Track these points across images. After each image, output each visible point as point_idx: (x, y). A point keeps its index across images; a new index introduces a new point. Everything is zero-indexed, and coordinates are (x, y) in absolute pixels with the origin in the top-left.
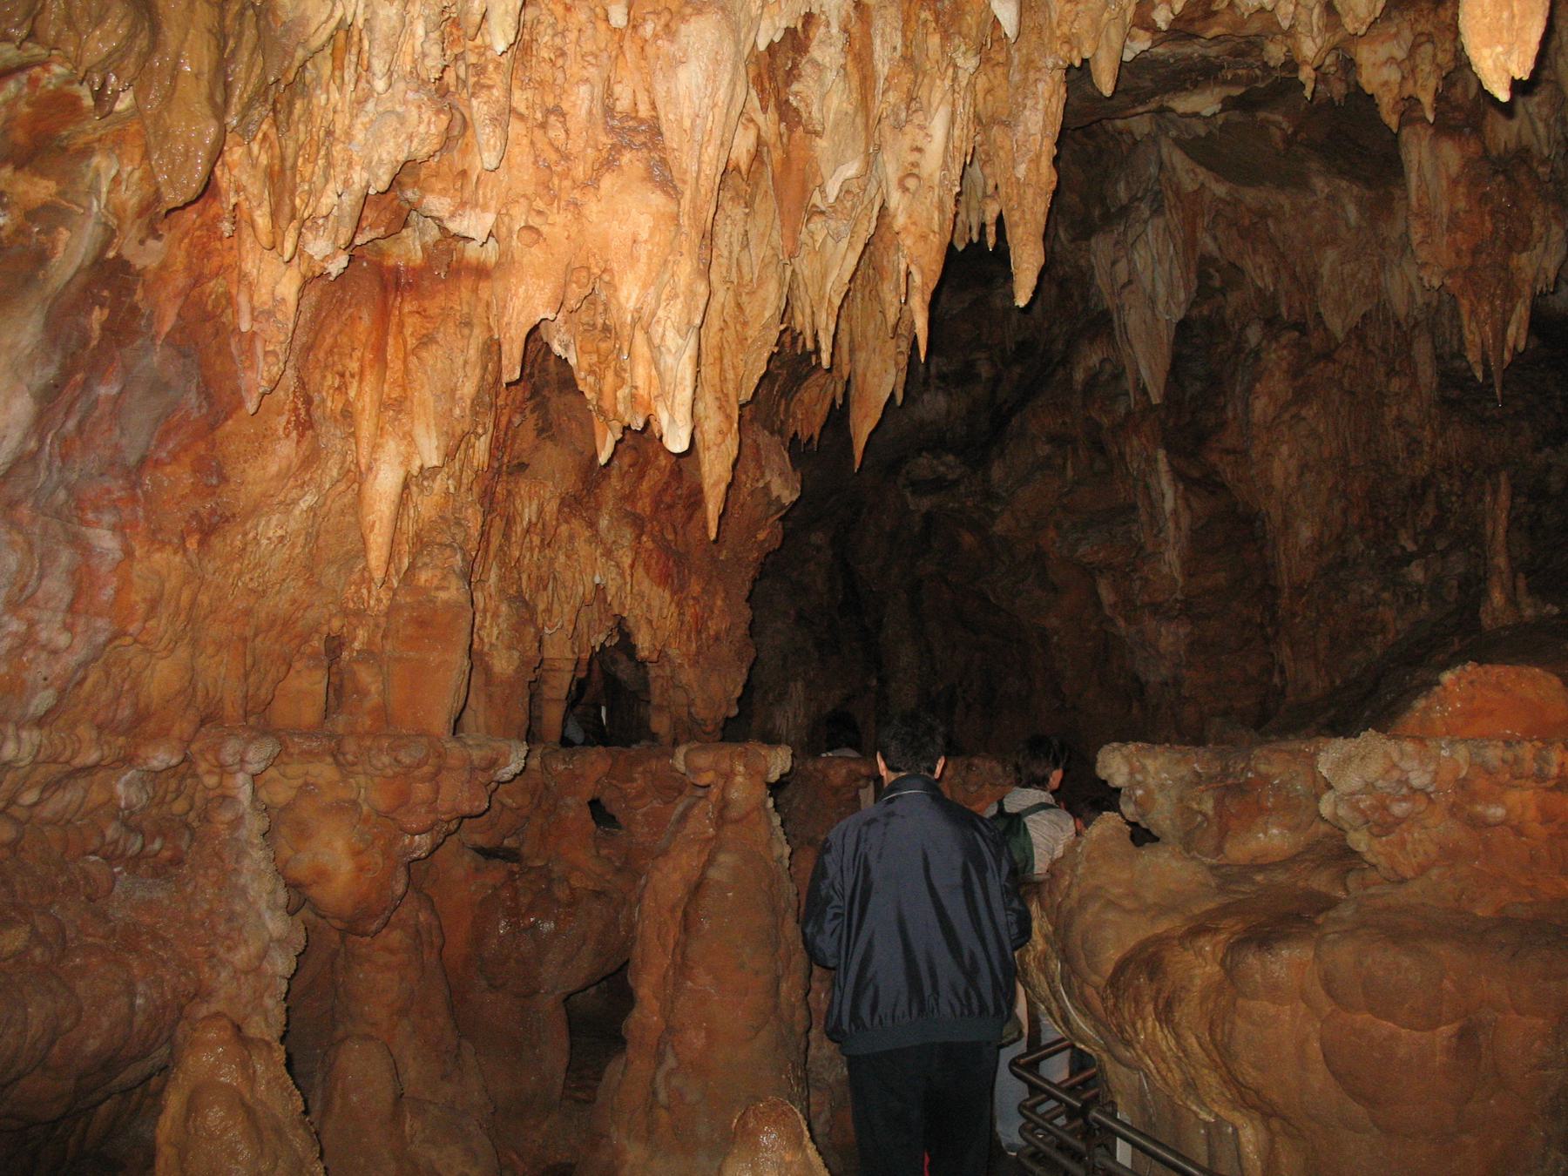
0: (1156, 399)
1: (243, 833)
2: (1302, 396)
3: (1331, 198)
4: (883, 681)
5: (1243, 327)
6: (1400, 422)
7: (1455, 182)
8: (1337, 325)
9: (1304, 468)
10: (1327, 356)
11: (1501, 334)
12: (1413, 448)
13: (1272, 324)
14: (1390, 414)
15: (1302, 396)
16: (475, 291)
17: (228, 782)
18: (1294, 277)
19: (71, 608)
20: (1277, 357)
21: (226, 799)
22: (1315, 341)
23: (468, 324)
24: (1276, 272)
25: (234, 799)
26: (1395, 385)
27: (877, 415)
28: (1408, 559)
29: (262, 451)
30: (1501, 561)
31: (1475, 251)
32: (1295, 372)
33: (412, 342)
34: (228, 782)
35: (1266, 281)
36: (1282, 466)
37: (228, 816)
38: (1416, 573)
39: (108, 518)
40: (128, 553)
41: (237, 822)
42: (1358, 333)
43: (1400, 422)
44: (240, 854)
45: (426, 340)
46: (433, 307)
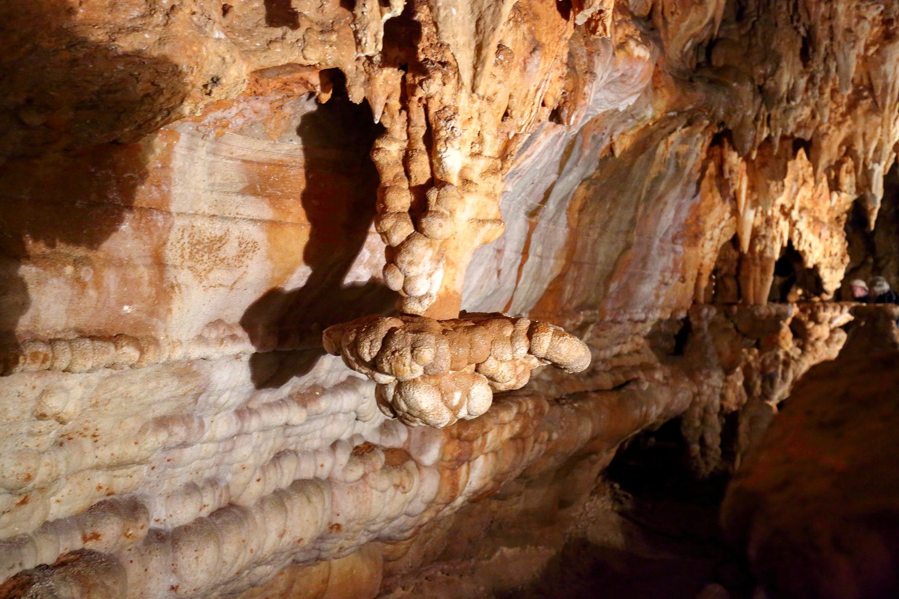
21: (700, 329)
41: (704, 337)
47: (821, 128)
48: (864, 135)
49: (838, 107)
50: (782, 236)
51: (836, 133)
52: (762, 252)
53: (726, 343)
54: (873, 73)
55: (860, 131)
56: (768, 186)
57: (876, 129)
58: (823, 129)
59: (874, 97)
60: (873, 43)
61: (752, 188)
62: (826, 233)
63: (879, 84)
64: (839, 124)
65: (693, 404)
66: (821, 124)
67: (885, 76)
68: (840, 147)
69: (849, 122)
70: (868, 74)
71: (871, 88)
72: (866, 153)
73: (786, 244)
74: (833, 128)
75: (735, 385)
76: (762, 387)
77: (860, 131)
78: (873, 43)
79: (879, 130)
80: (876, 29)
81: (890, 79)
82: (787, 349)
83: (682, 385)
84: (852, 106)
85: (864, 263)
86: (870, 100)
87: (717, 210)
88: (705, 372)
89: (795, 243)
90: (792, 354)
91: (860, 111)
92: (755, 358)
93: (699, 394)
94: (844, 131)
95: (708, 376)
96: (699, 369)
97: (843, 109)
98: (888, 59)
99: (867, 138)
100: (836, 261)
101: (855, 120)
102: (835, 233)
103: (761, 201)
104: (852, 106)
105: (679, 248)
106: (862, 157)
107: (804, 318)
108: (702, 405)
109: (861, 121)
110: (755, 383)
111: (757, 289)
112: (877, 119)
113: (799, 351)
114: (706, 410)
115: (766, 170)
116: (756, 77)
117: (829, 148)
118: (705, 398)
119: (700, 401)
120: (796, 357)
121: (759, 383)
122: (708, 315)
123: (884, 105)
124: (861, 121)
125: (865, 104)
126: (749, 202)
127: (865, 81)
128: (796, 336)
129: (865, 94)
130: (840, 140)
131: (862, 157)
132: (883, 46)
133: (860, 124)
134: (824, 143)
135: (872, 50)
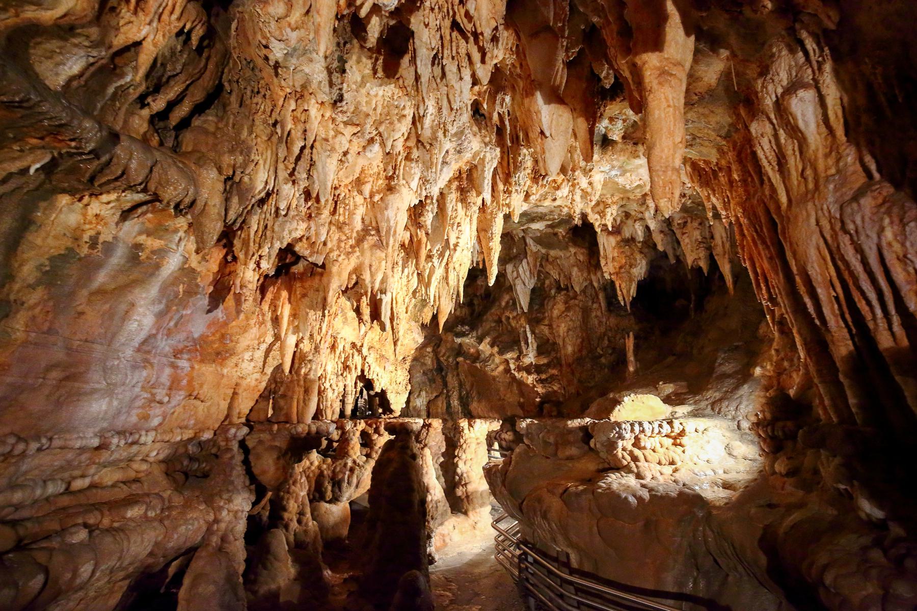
0: (526, 311)
1: (234, 461)
2: (568, 309)
3: (575, 253)
4: (448, 391)
5: (550, 290)
6: (596, 316)
7: (614, 248)
8: (577, 289)
9: (569, 330)
10: (575, 298)
11: (629, 291)
12: (600, 322)
13: (559, 289)
14: (594, 314)
15: (568, 309)
16: (320, 280)
17: (230, 444)
18: (565, 276)
19: (170, 389)
20: (560, 298)
21: (229, 450)
22: (571, 294)
23: (318, 291)
24: (559, 274)
25: (231, 450)
26: (595, 306)
27: (446, 317)
28: (601, 356)
29: (245, 331)
30: (632, 359)
31: (621, 268)
32: (566, 303)
33: (299, 296)
34: (230, 444)
35: (556, 277)
36: (562, 328)
37: (229, 455)
38: (603, 360)
39: (185, 356)
40: (192, 368)
41: (232, 457)
42: (584, 291)
43: (596, 316)
44: (233, 468)
45: (304, 296)
46: (307, 285)
47: (331, 255)
48: (371, 266)
49: (348, 238)
50: (356, 368)
51: (346, 261)
52: (306, 375)
53: (271, 462)
54: (379, 216)
55: (367, 262)
56: (307, 314)
57: (380, 263)
58: (334, 255)
59: (380, 237)
60: (378, 192)
61: (294, 315)
62: (392, 368)
63: (383, 226)
64: (348, 254)
65: (209, 531)
66: (331, 250)
67: (388, 220)
68: (350, 274)
69: (358, 254)
70: (376, 218)
71: (378, 231)
72: (373, 283)
73: (359, 374)
74: (343, 257)
75: (297, 495)
76: (332, 491)
77: (367, 262)
78: (378, 192)
79: (384, 263)
80: (380, 182)
81: (392, 223)
82: (355, 457)
83: (195, 515)
84: (360, 241)
85: (441, 393)
86: (376, 238)
87: (254, 332)
88: (225, 496)
89: (366, 373)
90: (358, 461)
91: (366, 245)
92: (329, 465)
93: (216, 521)
94: (353, 262)
95: (230, 501)
96: (219, 494)
97: (352, 242)
98: (390, 206)
99: (373, 269)
100: (401, 388)
101: (362, 252)
102: (399, 368)
103: (301, 327)
104: (360, 241)
105: (183, 363)
106: (369, 286)
107: (371, 431)
108: (220, 533)
109: (368, 254)
110: (326, 489)
111: (300, 407)
112: (380, 254)
113: (364, 458)
114: (224, 539)
115: (306, 301)
116: (225, 166)
117: (340, 274)
118: (223, 526)
119: (218, 530)
120: (361, 463)
121: (330, 488)
122: (235, 436)
123: (387, 244)
124: (368, 254)
125: (371, 240)
126: (291, 327)
127: (374, 224)
128: (363, 445)
129: (373, 233)
130: (350, 268)
131: (369, 286)
132: (385, 195)
133: (367, 256)
134: (335, 269)
135: (377, 198)
